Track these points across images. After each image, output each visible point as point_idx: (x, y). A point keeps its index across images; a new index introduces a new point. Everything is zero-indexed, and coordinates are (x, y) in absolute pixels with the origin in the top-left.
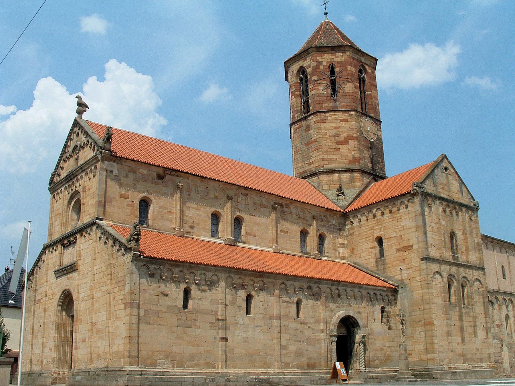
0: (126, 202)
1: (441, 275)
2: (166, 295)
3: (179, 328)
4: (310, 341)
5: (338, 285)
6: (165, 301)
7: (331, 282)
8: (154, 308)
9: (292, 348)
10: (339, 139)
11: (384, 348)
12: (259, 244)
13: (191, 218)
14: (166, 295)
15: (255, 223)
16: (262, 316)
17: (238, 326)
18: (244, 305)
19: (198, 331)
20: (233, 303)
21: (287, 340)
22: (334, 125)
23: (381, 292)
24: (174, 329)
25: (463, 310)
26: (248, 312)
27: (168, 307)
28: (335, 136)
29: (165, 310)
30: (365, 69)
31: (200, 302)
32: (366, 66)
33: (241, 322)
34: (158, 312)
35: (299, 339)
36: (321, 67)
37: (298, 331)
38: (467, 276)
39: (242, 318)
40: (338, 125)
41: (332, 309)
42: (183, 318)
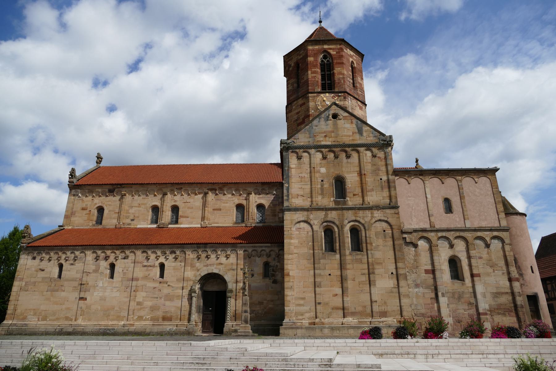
0: (85, 212)
1: (309, 224)
2: (43, 270)
3: (49, 293)
4: (169, 297)
5: (205, 247)
6: (41, 274)
7: (195, 245)
8: (33, 280)
9: (149, 303)
10: (299, 122)
11: (265, 302)
12: (191, 223)
13: (133, 213)
14: (43, 270)
15: (188, 208)
16: (120, 279)
17: (98, 288)
18: (108, 271)
19: (63, 294)
20: (96, 271)
21: (143, 297)
22: (296, 111)
23: (264, 248)
24: (45, 293)
25: (348, 258)
26: (112, 276)
27: (43, 278)
28: (297, 120)
29: (40, 280)
30: (329, 53)
31: (68, 273)
32: (329, 51)
33: (101, 285)
34: (35, 282)
35: (156, 296)
36: (291, 69)
37: (157, 289)
38: (358, 219)
39: (103, 282)
40: (299, 110)
41: (199, 268)
42: (53, 285)
